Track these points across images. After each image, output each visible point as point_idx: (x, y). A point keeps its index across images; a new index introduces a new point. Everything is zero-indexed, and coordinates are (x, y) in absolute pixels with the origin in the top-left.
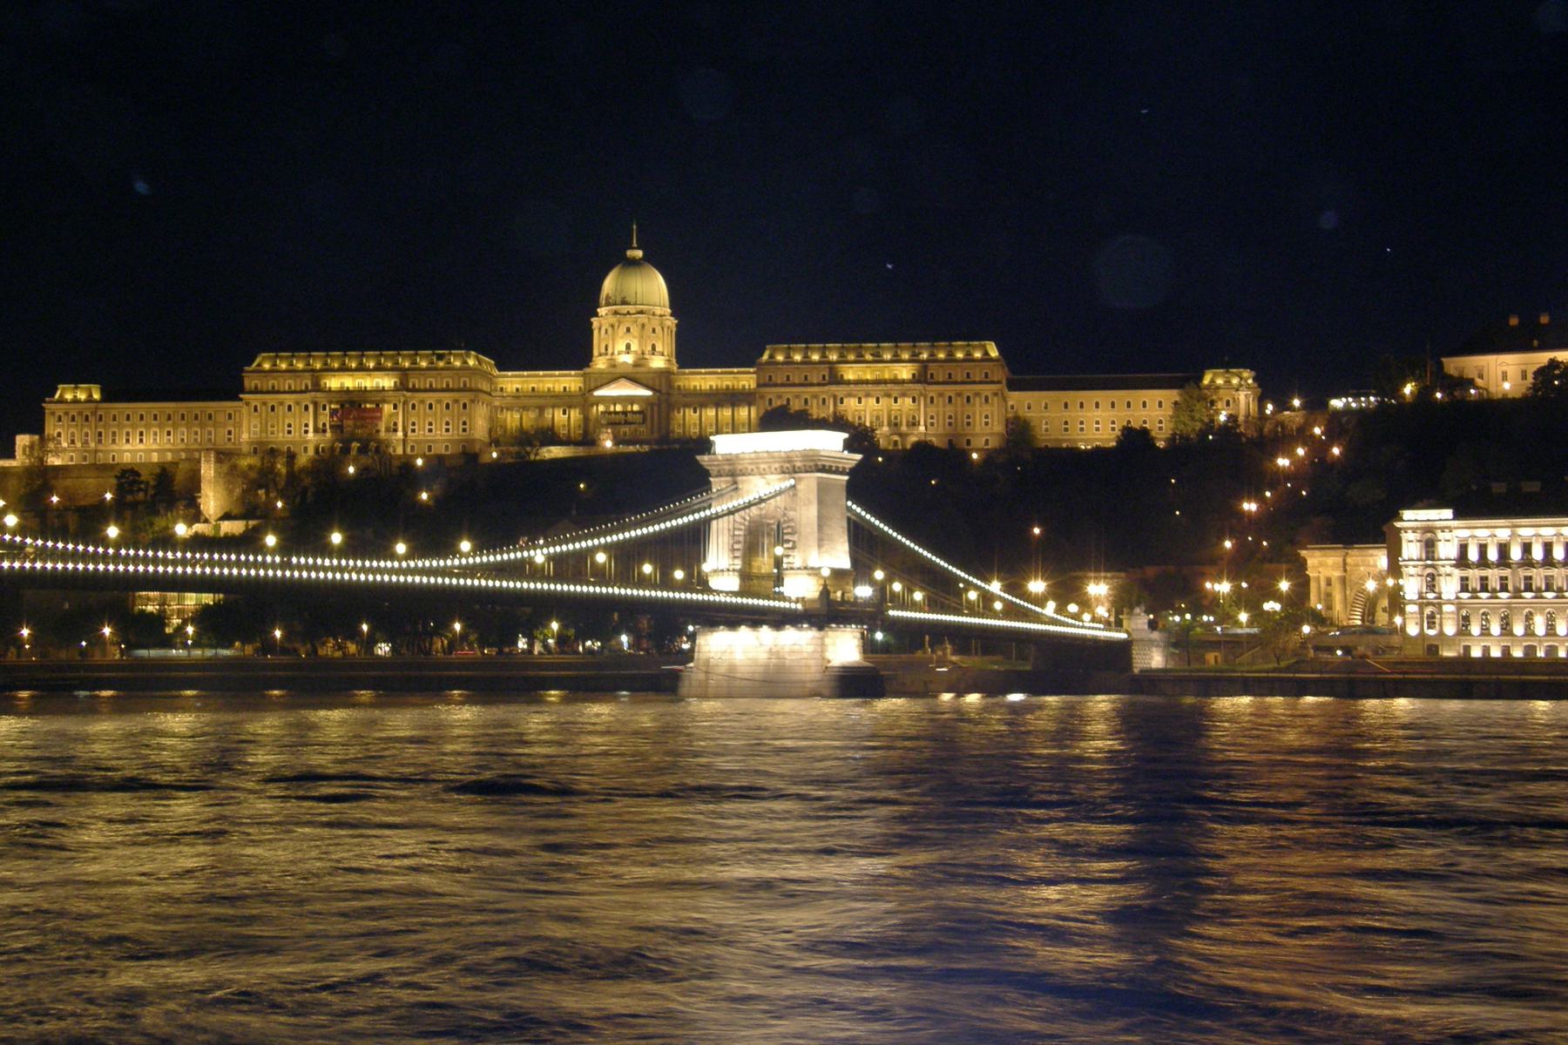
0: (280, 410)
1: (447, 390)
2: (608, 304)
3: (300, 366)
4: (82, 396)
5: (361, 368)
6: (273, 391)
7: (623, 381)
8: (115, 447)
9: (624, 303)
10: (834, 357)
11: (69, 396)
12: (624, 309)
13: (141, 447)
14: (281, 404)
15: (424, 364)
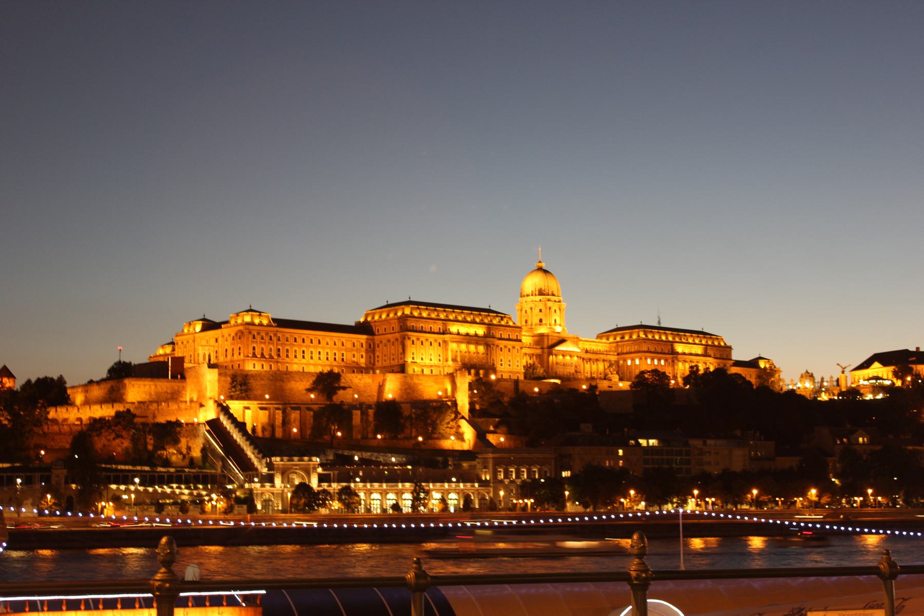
0: (427, 344)
1: (509, 340)
2: (541, 293)
3: (433, 315)
4: (265, 322)
5: (465, 321)
6: (422, 331)
7: (568, 343)
8: (287, 360)
9: (553, 295)
10: (670, 339)
11: (257, 321)
12: (552, 298)
13: (303, 361)
14: (427, 340)
15: (495, 322)
